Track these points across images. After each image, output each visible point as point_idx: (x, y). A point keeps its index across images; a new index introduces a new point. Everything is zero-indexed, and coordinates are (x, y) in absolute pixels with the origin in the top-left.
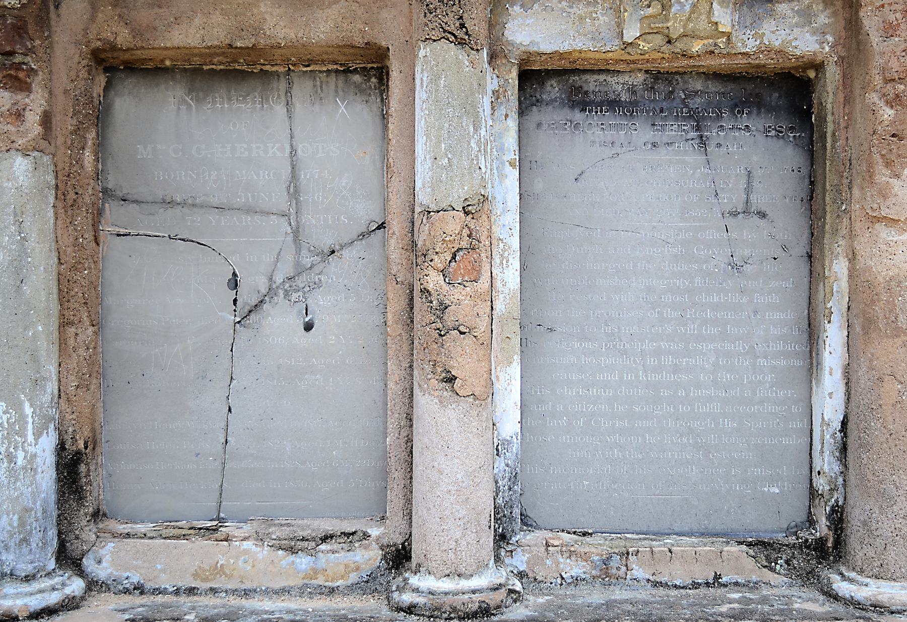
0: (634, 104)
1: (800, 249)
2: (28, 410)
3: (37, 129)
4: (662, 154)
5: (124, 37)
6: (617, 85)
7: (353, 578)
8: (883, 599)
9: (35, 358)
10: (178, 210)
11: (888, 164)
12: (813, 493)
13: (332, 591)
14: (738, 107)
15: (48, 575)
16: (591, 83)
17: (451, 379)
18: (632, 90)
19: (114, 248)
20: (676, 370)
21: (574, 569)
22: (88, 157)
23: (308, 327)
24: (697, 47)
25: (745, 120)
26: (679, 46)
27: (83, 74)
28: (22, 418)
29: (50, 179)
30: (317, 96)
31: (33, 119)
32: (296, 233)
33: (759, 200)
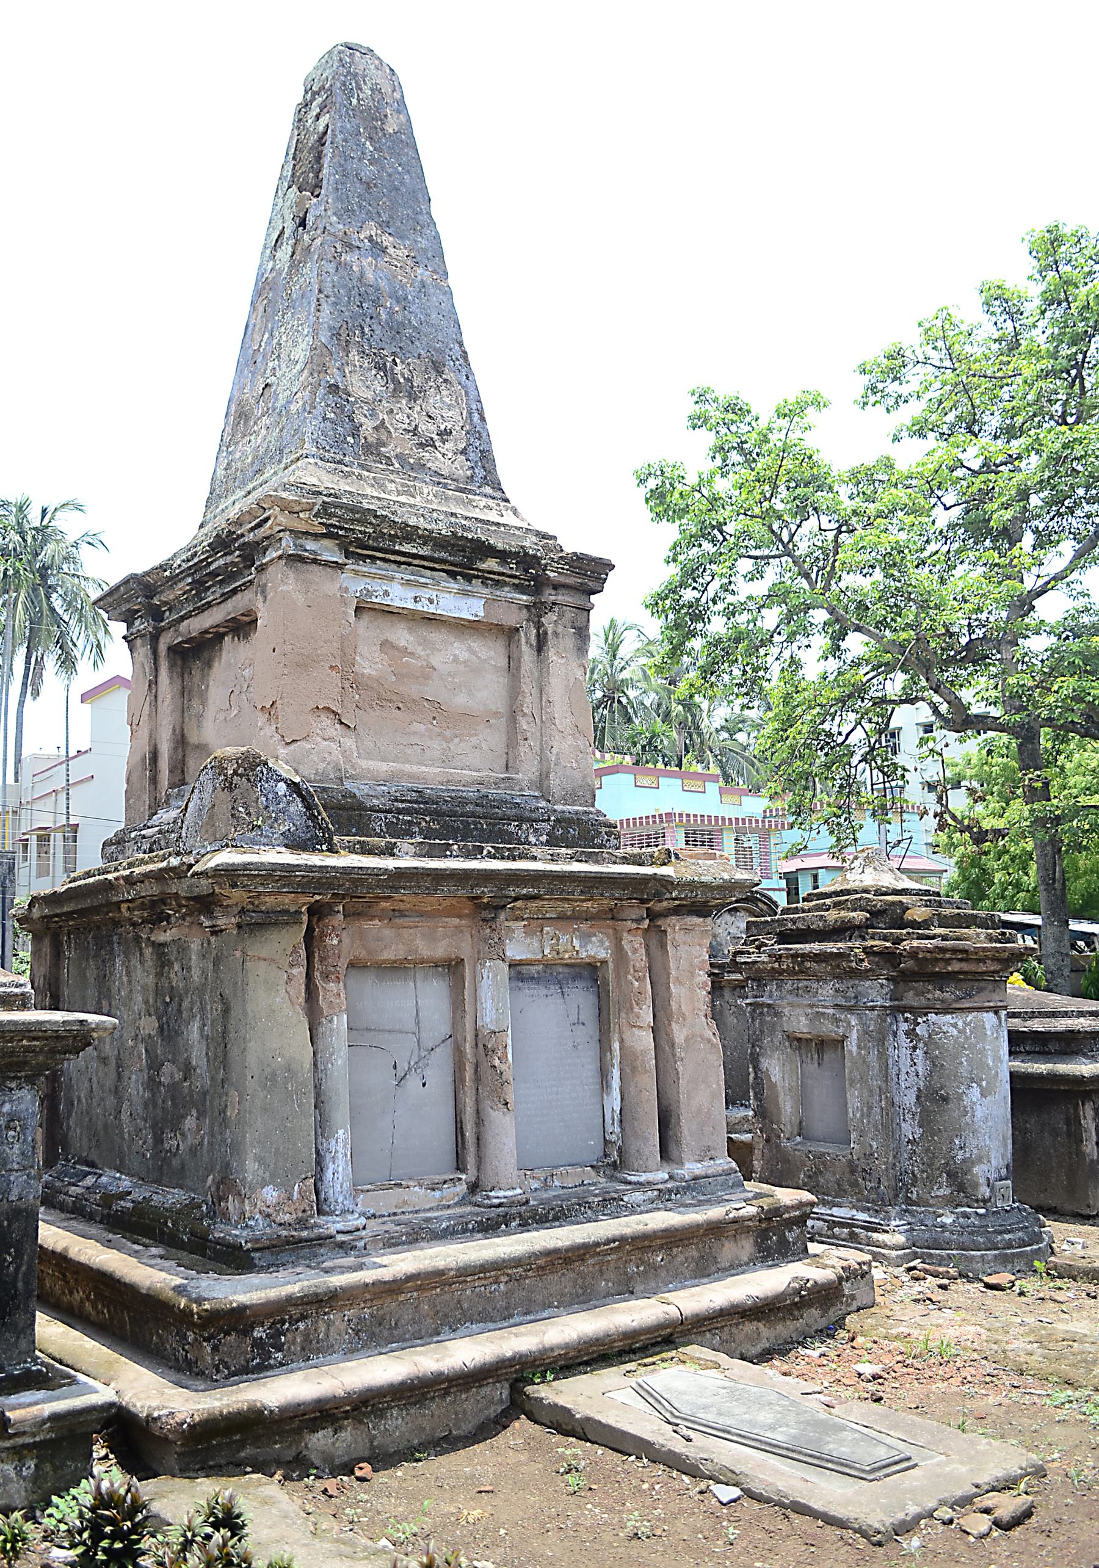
1: (597, 1038)
4: (550, 1000)
5: (363, 954)
7: (456, 1199)
8: (651, 1179)
10: (372, 1033)
11: (638, 1004)
12: (606, 1142)
13: (449, 1206)
14: (574, 979)
16: (524, 969)
17: (506, 1104)
18: (538, 972)
21: (535, 1185)
23: (424, 1085)
26: (561, 956)
30: (426, 978)
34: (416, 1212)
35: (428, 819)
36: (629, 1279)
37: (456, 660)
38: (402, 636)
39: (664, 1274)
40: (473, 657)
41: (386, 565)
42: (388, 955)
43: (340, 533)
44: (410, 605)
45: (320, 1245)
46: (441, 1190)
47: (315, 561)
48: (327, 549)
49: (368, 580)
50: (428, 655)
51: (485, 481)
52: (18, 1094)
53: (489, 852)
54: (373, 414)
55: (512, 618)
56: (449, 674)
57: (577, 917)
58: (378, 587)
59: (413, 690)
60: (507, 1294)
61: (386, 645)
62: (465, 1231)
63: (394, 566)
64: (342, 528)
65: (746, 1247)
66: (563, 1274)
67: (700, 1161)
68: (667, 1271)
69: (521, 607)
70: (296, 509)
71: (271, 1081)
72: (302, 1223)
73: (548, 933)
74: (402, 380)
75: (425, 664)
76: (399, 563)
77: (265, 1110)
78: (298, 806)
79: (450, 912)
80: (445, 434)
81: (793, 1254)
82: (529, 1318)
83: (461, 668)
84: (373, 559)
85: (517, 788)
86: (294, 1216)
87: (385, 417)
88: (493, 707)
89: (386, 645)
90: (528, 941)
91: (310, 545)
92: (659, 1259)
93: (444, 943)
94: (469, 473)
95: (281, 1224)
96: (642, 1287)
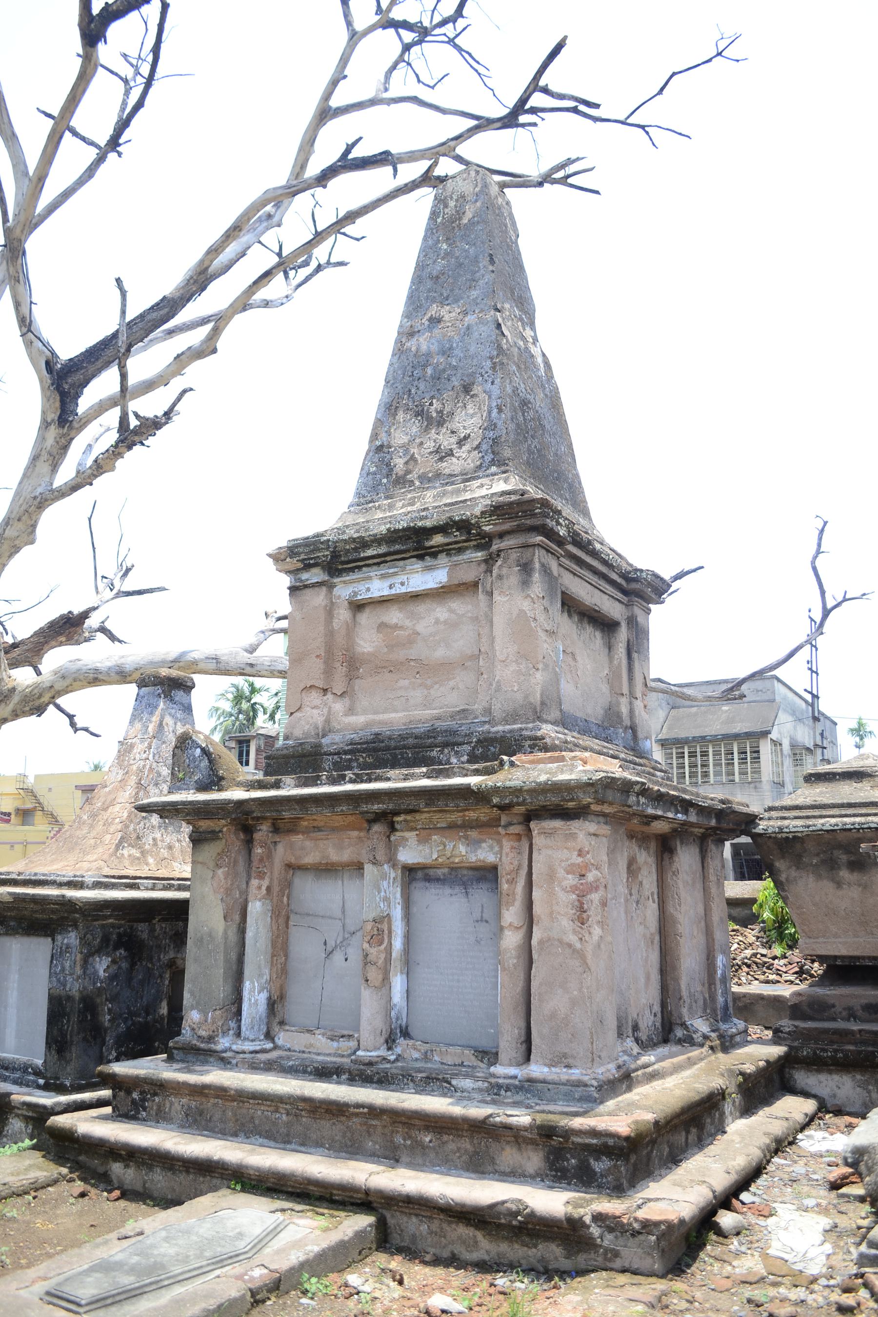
0: (445, 880)
2: (256, 984)
3: (265, 892)
5: (293, 861)
6: (440, 872)
9: (259, 967)
13: (343, 1056)
14: (479, 880)
15: (260, 1041)
17: (367, 981)
18: (444, 875)
19: (293, 930)
20: (458, 981)
21: (416, 1055)
22: (285, 899)
23: (346, 960)
24: (457, 860)
25: (481, 885)
26: (451, 860)
27: (283, 872)
28: (254, 987)
29: (270, 908)
31: (264, 888)
32: (344, 926)
33: (485, 916)
34: (319, 1054)
35: (364, 755)
36: (396, 1148)
37: (437, 621)
38: (394, 616)
39: (432, 1155)
40: (453, 615)
41: (369, 569)
42: (309, 859)
43: (311, 562)
44: (386, 592)
45: (211, 1055)
46: (338, 1041)
47: (306, 587)
48: (316, 575)
49: (355, 585)
50: (414, 625)
51: (492, 463)
52: (71, 934)
53: (351, 778)
54: (407, 451)
55: (469, 574)
56: (431, 635)
57: (467, 825)
58: (361, 587)
59: (401, 655)
60: (288, 1124)
61: (382, 626)
62: (305, 1072)
63: (375, 568)
64: (312, 559)
65: (534, 1160)
66: (334, 1124)
67: (550, 1066)
68: (437, 1153)
69: (479, 563)
70: (283, 557)
71: (200, 941)
72: (211, 1039)
73: (435, 841)
74: (434, 415)
75: (411, 632)
76: (378, 564)
77: (196, 960)
78: (205, 763)
79: (351, 827)
80: (461, 443)
81: (600, 1187)
82: (303, 1149)
83: (442, 627)
84: (359, 568)
85: (471, 717)
86: (208, 1033)
87: (416, 451)
88: (469, 652)
89: (382, 626)
90: (421, 848)
91: (305, 576)
92: (427, 1139)
93: (348, 851)
94: (478, 463)
95: (199, 1037)
96: (408, 1160)
